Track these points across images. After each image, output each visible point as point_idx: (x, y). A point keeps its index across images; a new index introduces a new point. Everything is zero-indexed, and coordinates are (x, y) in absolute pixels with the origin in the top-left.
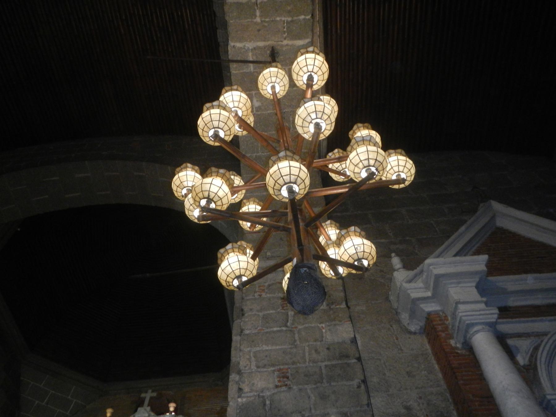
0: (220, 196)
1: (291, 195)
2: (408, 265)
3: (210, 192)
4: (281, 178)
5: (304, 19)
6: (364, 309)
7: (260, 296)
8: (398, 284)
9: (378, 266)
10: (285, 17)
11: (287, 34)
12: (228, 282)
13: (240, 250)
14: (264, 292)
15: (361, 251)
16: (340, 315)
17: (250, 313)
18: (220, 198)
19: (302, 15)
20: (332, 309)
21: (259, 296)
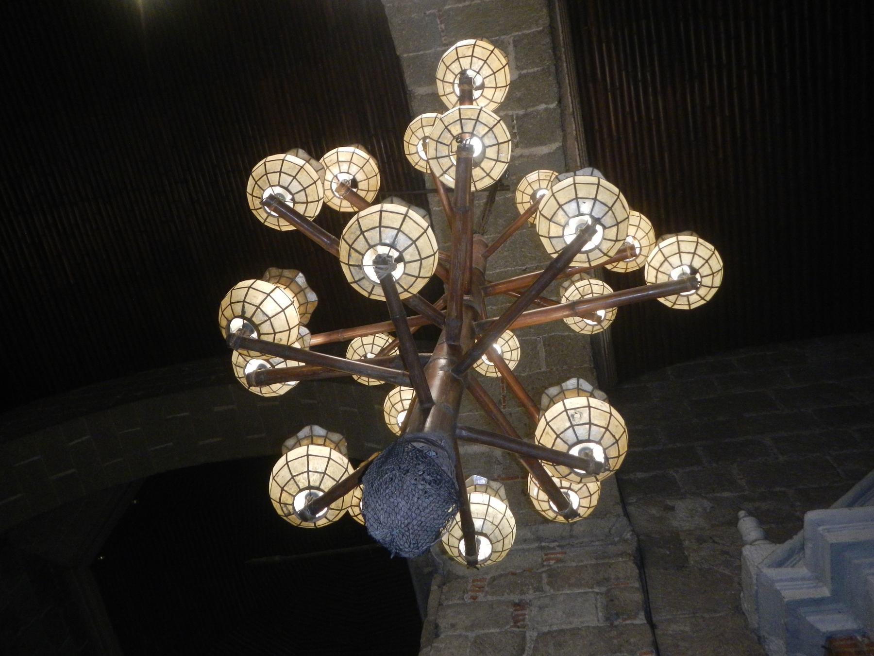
0: (266, 313)
1: (381, 269)
2: (774, 536)
3: (245, 303)
4: (361, 236)
5: (546, 110)
6: (687, 629)
7: (474, 598)
8: (753, 571)
9: (716, 543)
10: (512, 109)
11: (520, 138)
12: (286, 504)
13: (337, 448)
14: (483, 591)
15: (581, 423)
16: (632, 640)
17: (450, 633)
18: (267, 316)
19: (542, 103)
20: (616, 627)
21: (472, 600)
